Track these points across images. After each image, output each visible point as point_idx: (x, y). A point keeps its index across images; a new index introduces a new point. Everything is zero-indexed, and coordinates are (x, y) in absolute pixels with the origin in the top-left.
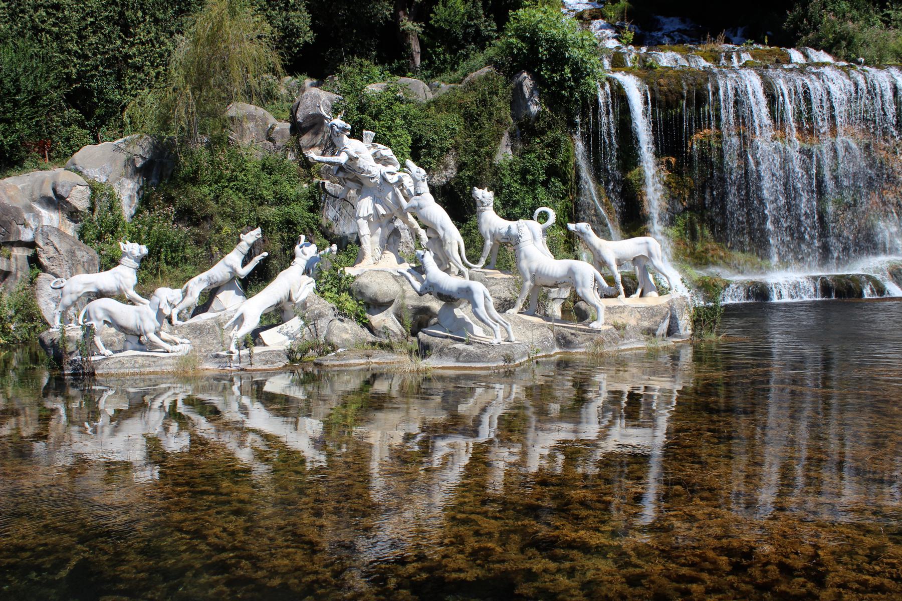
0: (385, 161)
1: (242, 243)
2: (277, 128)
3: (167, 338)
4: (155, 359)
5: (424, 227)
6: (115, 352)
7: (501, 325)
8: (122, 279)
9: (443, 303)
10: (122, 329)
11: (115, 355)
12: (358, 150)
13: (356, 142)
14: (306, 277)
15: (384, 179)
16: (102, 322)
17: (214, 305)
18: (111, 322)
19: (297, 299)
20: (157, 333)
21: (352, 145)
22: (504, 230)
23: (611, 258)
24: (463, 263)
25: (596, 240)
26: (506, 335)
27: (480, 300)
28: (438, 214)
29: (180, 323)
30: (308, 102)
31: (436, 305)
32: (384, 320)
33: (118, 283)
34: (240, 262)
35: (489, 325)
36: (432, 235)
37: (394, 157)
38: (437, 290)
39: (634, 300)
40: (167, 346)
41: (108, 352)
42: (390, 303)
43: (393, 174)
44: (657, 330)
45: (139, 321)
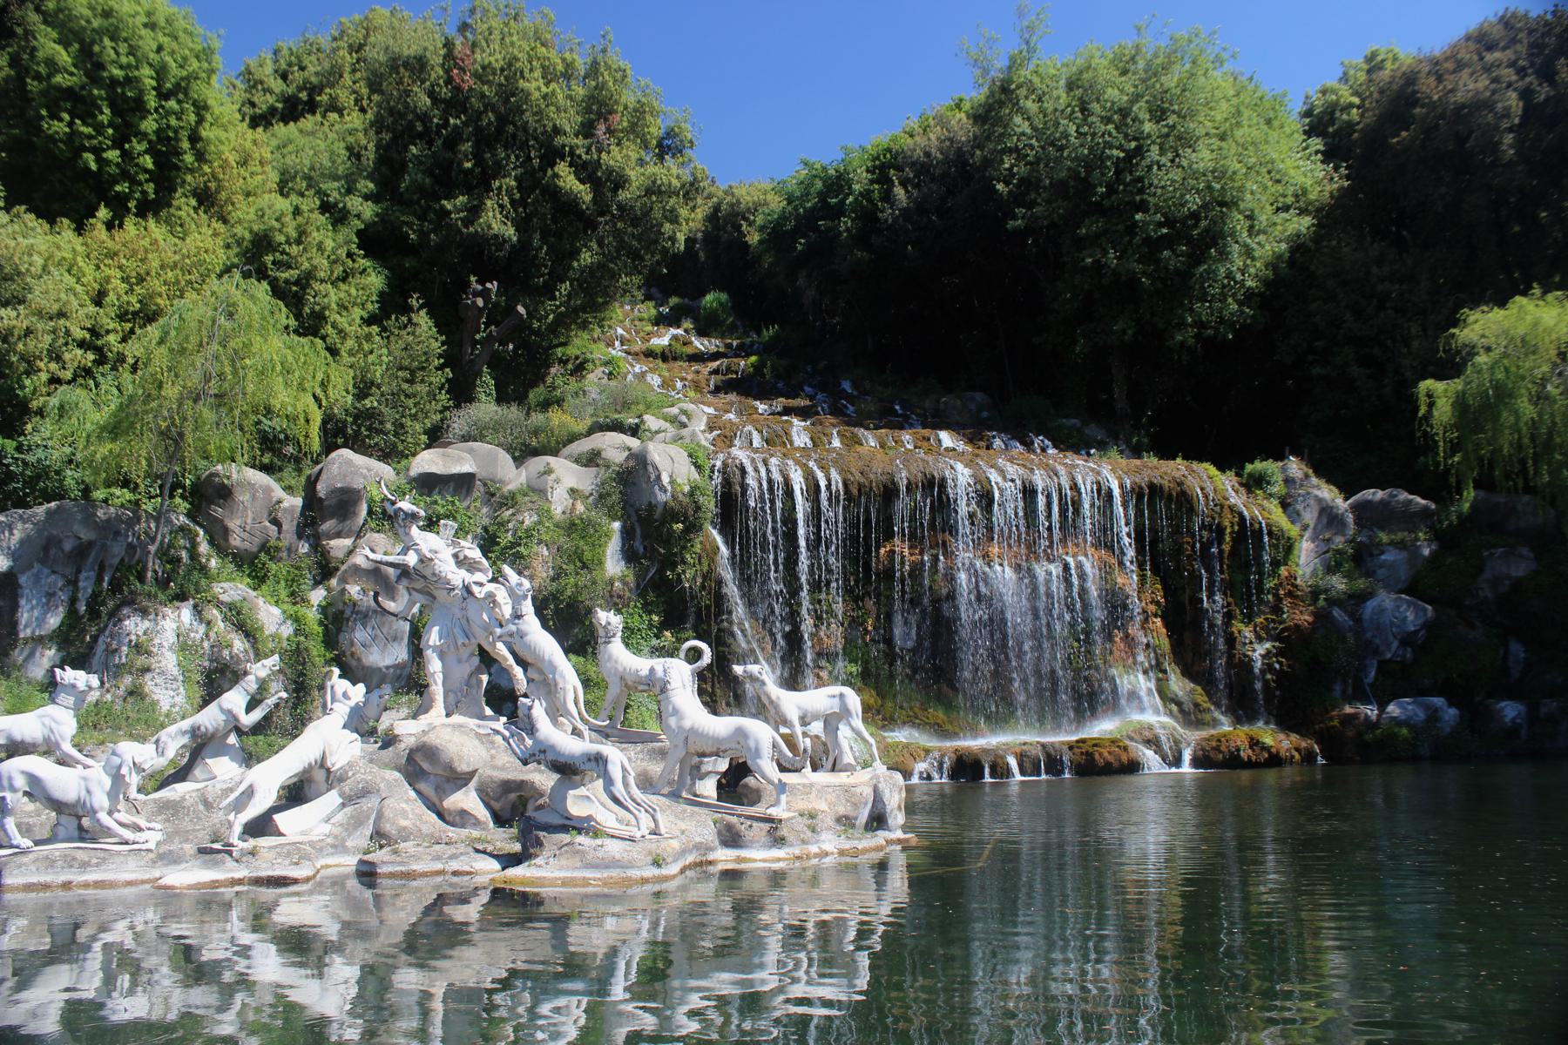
1: (251, 678)
2: (285, 504)
3: (125, 821)
4: (107, 854)
6: (37, 843)
8: (54, 725)
9: (556, 776)
10: (58, 806)
11: (35, 848)
13: (430, 536)
14: (347, 732)
15: (467, 589)
16: (21, 794)
17: (198, 772)
18: (36, 792)
20: (110, 813)
21: (427, 541)
22: (645, 672)
23: (793, 715)
24: (582, 719)
25: (774, 690)
26: (653, 825)
27: (615, 772)
28: (546, 645)
29: (141, 797)
30: (335, 469)
31: (544, 779)
32: (467, 800)
33: (46, 732)
35: (627, 809)
36: (535, 676)
37: (484, 561)
38: (550, 757)
39: (822, 777)
40: (128, 834)
41: (26, 843)
42: (472, 774)
43: (481, 585)
44: (856, 818)
45: (83, 793)
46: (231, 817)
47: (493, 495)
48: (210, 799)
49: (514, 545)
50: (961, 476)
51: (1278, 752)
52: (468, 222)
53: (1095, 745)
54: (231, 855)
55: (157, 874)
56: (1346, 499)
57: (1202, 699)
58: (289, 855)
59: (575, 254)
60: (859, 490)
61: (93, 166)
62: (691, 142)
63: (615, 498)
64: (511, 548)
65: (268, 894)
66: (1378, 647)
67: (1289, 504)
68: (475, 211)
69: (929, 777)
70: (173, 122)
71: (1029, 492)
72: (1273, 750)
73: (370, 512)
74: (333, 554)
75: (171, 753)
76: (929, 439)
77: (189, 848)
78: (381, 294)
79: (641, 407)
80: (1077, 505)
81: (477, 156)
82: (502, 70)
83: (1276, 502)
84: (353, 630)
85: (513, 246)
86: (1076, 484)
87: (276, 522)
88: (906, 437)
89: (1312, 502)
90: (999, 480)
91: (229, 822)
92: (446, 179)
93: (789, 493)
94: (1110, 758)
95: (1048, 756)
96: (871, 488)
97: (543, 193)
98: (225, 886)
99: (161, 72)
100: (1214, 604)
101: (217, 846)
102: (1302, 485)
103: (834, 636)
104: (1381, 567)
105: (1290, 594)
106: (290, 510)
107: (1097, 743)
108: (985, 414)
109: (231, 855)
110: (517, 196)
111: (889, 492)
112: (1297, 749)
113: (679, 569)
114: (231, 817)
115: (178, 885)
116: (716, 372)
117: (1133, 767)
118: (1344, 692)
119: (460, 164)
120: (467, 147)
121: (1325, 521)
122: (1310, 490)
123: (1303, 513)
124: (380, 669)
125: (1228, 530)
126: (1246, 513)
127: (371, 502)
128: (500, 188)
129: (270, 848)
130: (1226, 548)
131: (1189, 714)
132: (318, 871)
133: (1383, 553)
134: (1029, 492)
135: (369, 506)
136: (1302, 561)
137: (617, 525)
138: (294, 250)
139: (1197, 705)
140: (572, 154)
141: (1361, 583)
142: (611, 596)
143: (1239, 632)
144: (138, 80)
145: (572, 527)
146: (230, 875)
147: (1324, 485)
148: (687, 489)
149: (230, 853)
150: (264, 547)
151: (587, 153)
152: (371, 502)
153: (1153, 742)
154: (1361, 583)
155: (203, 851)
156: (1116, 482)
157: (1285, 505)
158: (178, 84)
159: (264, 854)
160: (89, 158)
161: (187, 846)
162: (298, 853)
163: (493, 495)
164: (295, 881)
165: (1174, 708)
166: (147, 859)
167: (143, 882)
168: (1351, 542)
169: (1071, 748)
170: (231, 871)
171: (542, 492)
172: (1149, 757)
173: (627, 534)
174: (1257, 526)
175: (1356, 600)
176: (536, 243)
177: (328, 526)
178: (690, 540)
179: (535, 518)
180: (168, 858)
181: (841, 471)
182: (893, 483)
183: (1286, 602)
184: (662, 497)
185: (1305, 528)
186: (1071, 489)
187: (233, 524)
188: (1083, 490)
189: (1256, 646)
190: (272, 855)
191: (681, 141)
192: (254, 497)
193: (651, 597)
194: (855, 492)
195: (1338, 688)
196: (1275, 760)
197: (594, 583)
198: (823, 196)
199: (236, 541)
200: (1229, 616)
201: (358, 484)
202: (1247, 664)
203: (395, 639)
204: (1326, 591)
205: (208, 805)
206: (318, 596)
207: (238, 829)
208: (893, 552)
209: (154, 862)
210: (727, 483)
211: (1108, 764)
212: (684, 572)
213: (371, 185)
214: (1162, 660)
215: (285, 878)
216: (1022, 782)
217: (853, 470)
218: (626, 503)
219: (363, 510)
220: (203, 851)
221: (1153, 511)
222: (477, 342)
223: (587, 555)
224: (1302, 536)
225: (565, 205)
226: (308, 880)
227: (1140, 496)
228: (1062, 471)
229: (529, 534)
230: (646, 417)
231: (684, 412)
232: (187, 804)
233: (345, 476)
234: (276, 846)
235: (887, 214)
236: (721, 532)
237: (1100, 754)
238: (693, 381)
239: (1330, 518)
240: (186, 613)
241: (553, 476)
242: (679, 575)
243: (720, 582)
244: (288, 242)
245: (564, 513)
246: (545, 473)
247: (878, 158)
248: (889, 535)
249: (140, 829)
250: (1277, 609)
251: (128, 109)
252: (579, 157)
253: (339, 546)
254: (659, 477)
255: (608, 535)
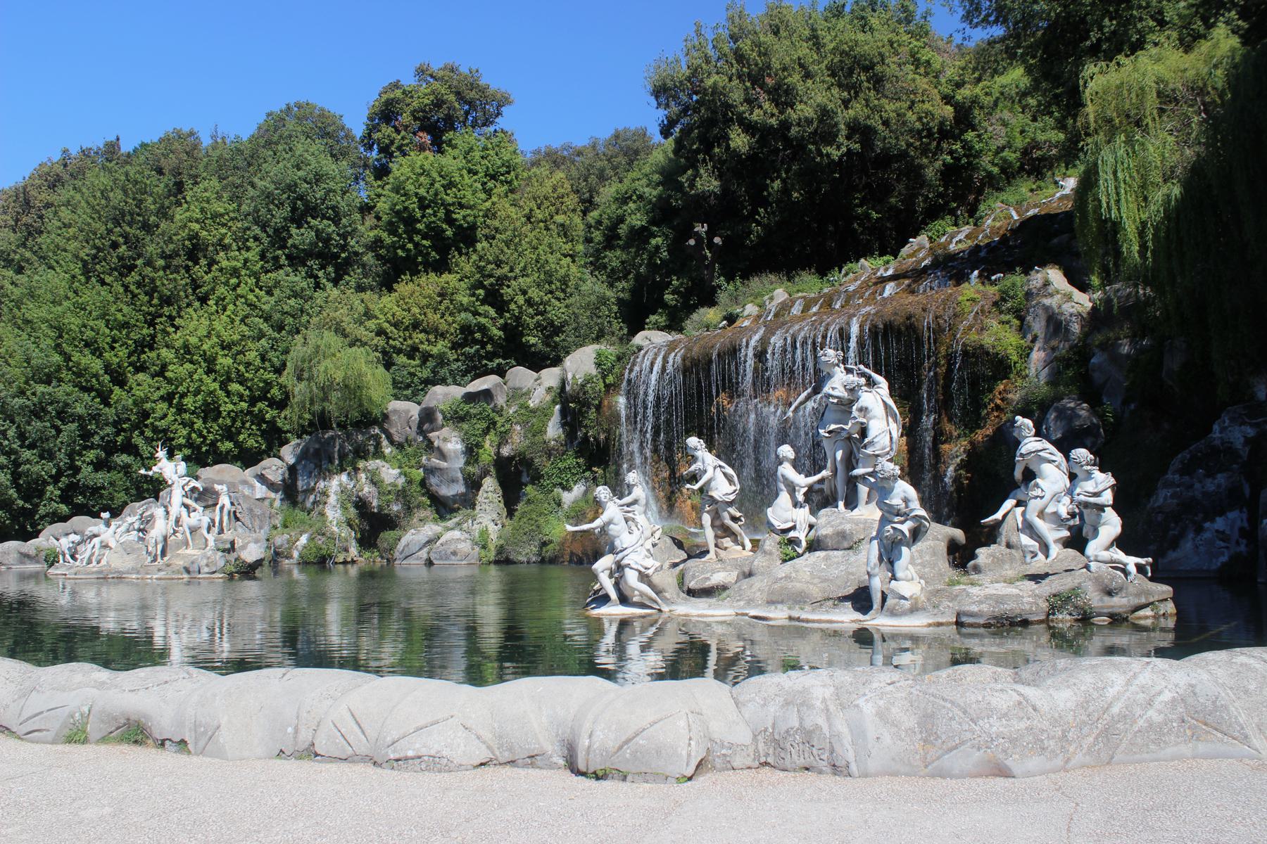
68: (697, 175)
70: (433, 219)
89: (1040, 312)
127: (442, 412)
137: (558, 407)
138: (490, 267)
152: (442, 412)
160: (400, 252)
187: (393, 431)
192: (400, 417)
194: (688, 363)
201: (432, 405)
203: (453, 481)
212: (588, 432)
219: (440, 417)
240: (344, 477)
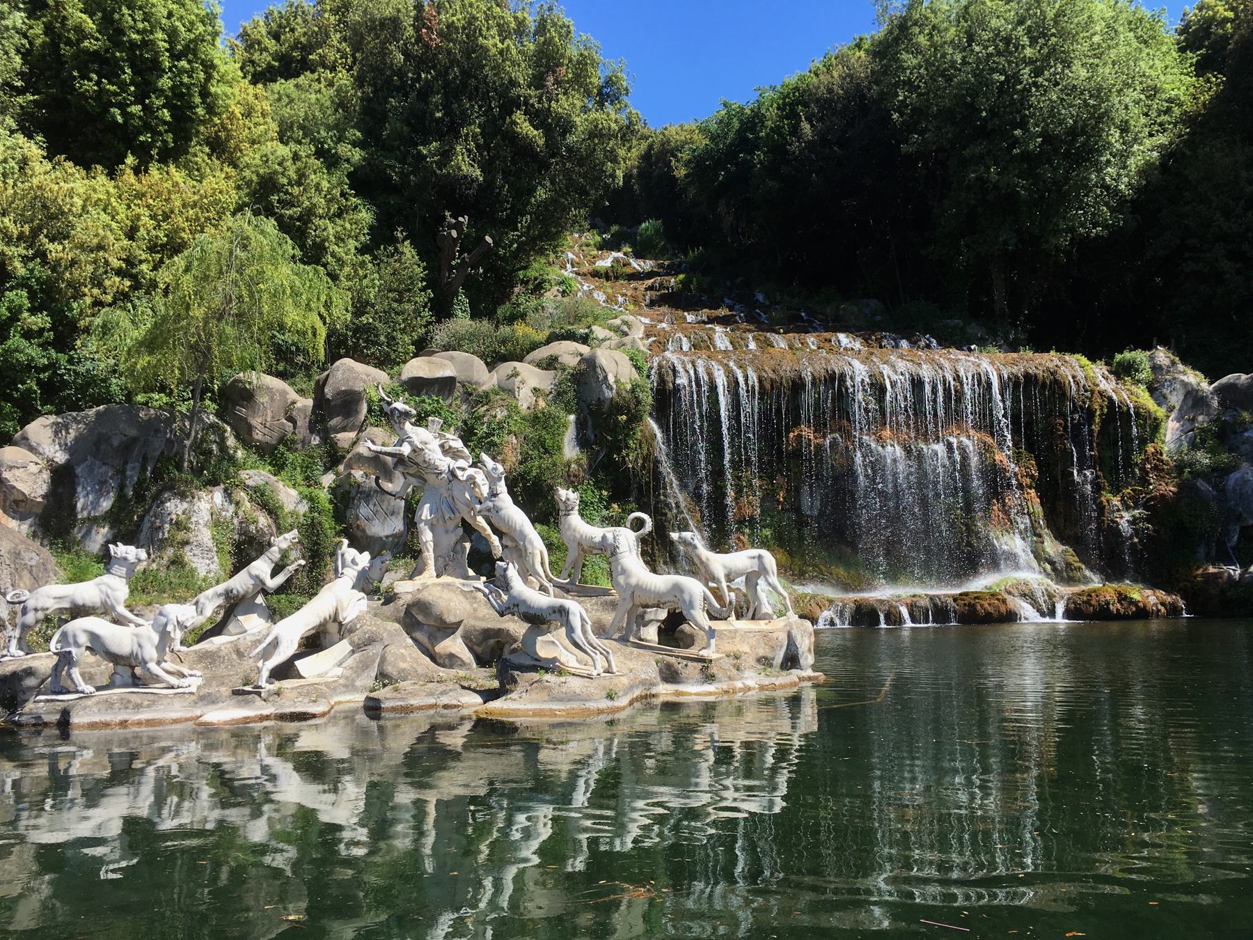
0: (455, 454)
1: (275, 549)
2: (299, 405)
3: (171, 670)
5: (496, 531)
6: (98, 689)
7: (601, 653)
8: (109, 591)
9: (527, 625)
10: (114, 658)
11: (97, 693)
12: (424, 439)
14: (355, 591)
15: (452, 473)
16: (84, 648)
17: (231, 627)
19: (344, 619)
20: (158, 663)
21: (418, 435)
22: (598, 539)
23: (720, 574)
24: (547, 576)
25: (704, 552)
26: (607, 665)
27: (576, 622)
29: (184, 649)
30: (339, 375)
31: (517, 628)
32: (454, 645)
33: (103, 597)
34: (269, 572)
35: (585, 652)
36: (509, 543)
37: (465, 450)
38: (522, 609)
39: (744, 625)
40: (173, 680)
41: (89, 689)
44: (773, 659)
45: (136, 648)
46: (260, 664)
47: (471, 394)
48: (242, 650)
49: (488, 435)
50: (859, 371)
51: (1145, 606)
52: (441, 165)
53: (976, 598)
54: (260, 696)
55: (198, 713)
56: (1211, 383)
57: (1073, 559)
58: (308, 694)
59: (531, 191)
60: (772, 385)
61: (120, 119)
62: (627, 89)
63: (571, 395)
64: (486, 438)
65: (290, 727)
66: (1241, 514)
67: (1156, 389)
68: (446, 155)
69: (832, 623)
70: (186, 80)
71: (917, 384)
72: (1141, 605)
73: (370, 411)
74: (340, 444)
75: (208, 612)
76: (830, 341)
77: (225, 691)
78: (371, 228)
79: (590, 319)
80: (960, 395)
81: (446, 107)
82: (464, 28)
83: (1143, 387)
84: (358, 507)
85: (480, 185)
86: (958, 376)
87: (291, 419)
88: (811, 339)
90: (891, 373)
91: (258, 668)
92: (421, 127)
93: (713, 388)
94: (990, 609)
95: (935, 605)
96: (781, 383)
97: (504, 137)
98: (255, 722)
99: (172, 35)
100: (1082, 477)
101: (248, 688)
102: (1169, 371)
103: (753, 505)
104: (1243, 443)
105: (1155, 468)
106: (304, 408)
107: (978, 596)
108: (878, 318)
109: (260, 696)
110: (482, 141)
111: (797, 385)
112: (1163, 604)
113: (624, 452)
114: (260, 664)
115: (215, 721)
116: (651, 288)
117: (1011, 617)
118: (1207, 554)
119: (432, 114)
120: (437, 98)
121: (1190, 402)
122: (1176, 376)
123: (1169, 396)
124: (381, 538)
125: (1098, 413)
126: (1115, 397)
128: (467, 134)
129: (292, 688)
130: (1096, 428)
131: (1061, 572)
132: (332, 708)
133: (1246, 430)
134: (917, 384)
135: (369, 405)
136: (1168, 438)
137: (572, 417)
138: (296, 190)
139: (1068, 565)
140: (526, 103)
141: (1224, 457)
142: (569, 476)
143: (1108, 501)
144: (153, 43)
145: (537, 420)
146: (259, 712)
147: (1189, 371)
148: (629, 387)
149: (259, 694)
150: (282, 440)
151: (539, 103)
153: (1029, 596)
154: (1224, 457)
155: (236, 693)
156: (995, 373)
157: (1152, 389)
158: (187, 47)
159: (287, 694)
160: (116, 111)
161: (223, 689)
162: (315, 692)
163: (471, 394)
164: (314, 716)
165: (1048, 567)
166: (189, 701)
167: (187, 720)
168: (1215, 421)
169: (955, 600)
170: (261, 708)
171: (511, 392)
172: (1026, 610)
173: (580, 425)
174: (1125, 409)
175: (1218, 473)
176: (499, 182)
177: (334, 422)
178: (632, 429)
179: (505, 413)
180: (207, 699)
181: (757, 370)
182: (800, 378)
183: (1152, 477)
184: (609, 394)
185: (1171, 409)
186: (954, 380)
187: (256, 421)
188: (965, 380)
189: (1124, 514)
190: (295, 694)
191: (618, 89)
192: (272, 399)
193: (601, 476)
194: (768, 386)
195: (1202, 551)
196: (1142, 613)
197: (555, 465)
198: (741, 132)
199: (258, 435)
200: (1097, 488)
201: (358, 387)
202: (1114, 531)
203: (393, 513)
204: (1191, 465)
205: (240, 654)
206: (328, 479)
207: (265, 674)
208: (800, 436)
209: (196, 703)
210: (662, 380)
211: (988, 614)
212: (628, 455)
213: (358, 134)
214: (1036, 525)
215: (305, 714)
216: (912, 628)
217: (767, 369)
218: (579, 397)
220: (236, 693)
221: (1028, 397)
222: (453, 268)
223: (549, 443)
224: (1168, 417)
225: (523, 148)
226: (323, 715)
227: (1016, 384)
228: (947, 364)
229: (500, 426)
230: (594, 328)
231: (625, 323)
232: (222, 654)
233: (348, 381)
234: (297, 688)
235: (795, 147)
236: (658, 421)
237: (982, 606)
238: (632, 296)
239: (1194, 400)
240: (218, 496)
241: (519, 378)
242: (623, 458)
243: (657, 462)
244: (290, 184)
245: (529, 408)
246: (512, 376)
247: (788, 96)
248: (797, 423)
249: (183, 676)
250: (1144, 482)
251: (147, 69)
252: (533, 105)
253: (345, 438)
254: (606, 377)
255: (565, 426)
